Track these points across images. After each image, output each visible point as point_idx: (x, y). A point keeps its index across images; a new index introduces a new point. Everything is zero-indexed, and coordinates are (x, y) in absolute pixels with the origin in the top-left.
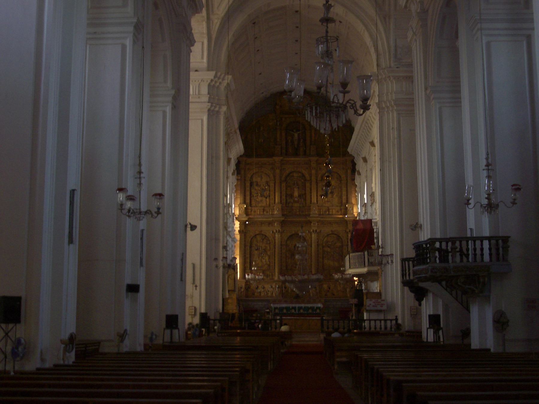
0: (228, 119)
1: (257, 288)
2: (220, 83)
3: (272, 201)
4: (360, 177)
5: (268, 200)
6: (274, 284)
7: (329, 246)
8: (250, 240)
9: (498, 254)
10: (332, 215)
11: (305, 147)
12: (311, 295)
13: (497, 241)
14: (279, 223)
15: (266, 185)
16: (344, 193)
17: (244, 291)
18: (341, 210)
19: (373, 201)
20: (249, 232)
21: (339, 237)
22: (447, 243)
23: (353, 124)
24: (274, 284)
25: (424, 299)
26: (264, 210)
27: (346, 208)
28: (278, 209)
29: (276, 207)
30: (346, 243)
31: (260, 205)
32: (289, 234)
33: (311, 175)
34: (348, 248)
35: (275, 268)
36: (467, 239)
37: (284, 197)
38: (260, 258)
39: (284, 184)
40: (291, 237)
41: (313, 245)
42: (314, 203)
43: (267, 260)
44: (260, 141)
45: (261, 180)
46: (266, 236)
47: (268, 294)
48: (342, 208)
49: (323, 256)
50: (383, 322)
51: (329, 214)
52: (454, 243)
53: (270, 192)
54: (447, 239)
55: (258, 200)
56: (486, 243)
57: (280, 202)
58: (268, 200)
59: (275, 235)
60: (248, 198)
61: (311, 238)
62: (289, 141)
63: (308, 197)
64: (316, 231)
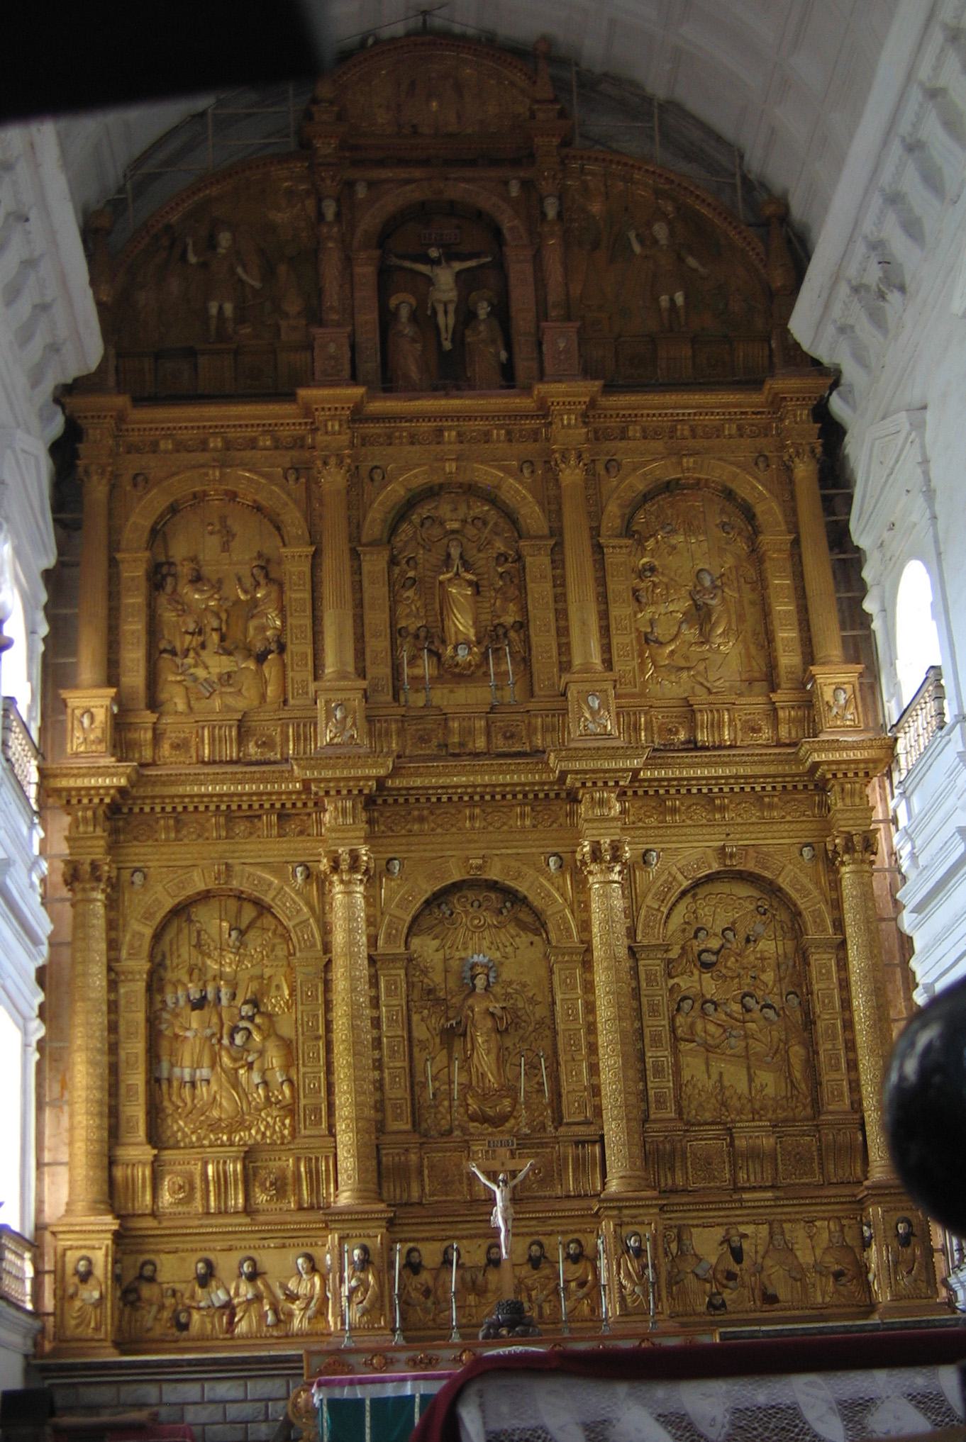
1: (205, 1279)
3: (300, 673)
6: (332, 1239)
7: (705, 957)
8: (148, 932)
10: (720, 747)
11: (509, 347)
14: (349, 804)
16: (783, 607)
17: (102, 1297)
18: (773, 713)
20: (138, 878)
21: (772, 889)
24: (332, 1239)
26: (243, 731)
27: (808, 704)
28: (345, 718)
29: (328, 702)
30: (831, 931)
31: (217, 703)
32: (428, 889)
33: (553, 506)
34: (843, 965)
35: (331, 1127)
37: (378, 645)
38: (226, 1060)
39: (375, 563)
41: (598, 953)
42: (587, 668)
43: (279, 1078)
44: (214, 310)
45: (225, 547)
46: (262, 908)
47: (290, 1315)
49: (673, 1030)
51: (693, 745)
53: (283, 622)
55: (201, 673)
57: (351, 669)
58: (270, 669)
59: (324, 894)
60: (134, 657)
61: (582, 906)
62: (404, 313)
63: (543, 640)
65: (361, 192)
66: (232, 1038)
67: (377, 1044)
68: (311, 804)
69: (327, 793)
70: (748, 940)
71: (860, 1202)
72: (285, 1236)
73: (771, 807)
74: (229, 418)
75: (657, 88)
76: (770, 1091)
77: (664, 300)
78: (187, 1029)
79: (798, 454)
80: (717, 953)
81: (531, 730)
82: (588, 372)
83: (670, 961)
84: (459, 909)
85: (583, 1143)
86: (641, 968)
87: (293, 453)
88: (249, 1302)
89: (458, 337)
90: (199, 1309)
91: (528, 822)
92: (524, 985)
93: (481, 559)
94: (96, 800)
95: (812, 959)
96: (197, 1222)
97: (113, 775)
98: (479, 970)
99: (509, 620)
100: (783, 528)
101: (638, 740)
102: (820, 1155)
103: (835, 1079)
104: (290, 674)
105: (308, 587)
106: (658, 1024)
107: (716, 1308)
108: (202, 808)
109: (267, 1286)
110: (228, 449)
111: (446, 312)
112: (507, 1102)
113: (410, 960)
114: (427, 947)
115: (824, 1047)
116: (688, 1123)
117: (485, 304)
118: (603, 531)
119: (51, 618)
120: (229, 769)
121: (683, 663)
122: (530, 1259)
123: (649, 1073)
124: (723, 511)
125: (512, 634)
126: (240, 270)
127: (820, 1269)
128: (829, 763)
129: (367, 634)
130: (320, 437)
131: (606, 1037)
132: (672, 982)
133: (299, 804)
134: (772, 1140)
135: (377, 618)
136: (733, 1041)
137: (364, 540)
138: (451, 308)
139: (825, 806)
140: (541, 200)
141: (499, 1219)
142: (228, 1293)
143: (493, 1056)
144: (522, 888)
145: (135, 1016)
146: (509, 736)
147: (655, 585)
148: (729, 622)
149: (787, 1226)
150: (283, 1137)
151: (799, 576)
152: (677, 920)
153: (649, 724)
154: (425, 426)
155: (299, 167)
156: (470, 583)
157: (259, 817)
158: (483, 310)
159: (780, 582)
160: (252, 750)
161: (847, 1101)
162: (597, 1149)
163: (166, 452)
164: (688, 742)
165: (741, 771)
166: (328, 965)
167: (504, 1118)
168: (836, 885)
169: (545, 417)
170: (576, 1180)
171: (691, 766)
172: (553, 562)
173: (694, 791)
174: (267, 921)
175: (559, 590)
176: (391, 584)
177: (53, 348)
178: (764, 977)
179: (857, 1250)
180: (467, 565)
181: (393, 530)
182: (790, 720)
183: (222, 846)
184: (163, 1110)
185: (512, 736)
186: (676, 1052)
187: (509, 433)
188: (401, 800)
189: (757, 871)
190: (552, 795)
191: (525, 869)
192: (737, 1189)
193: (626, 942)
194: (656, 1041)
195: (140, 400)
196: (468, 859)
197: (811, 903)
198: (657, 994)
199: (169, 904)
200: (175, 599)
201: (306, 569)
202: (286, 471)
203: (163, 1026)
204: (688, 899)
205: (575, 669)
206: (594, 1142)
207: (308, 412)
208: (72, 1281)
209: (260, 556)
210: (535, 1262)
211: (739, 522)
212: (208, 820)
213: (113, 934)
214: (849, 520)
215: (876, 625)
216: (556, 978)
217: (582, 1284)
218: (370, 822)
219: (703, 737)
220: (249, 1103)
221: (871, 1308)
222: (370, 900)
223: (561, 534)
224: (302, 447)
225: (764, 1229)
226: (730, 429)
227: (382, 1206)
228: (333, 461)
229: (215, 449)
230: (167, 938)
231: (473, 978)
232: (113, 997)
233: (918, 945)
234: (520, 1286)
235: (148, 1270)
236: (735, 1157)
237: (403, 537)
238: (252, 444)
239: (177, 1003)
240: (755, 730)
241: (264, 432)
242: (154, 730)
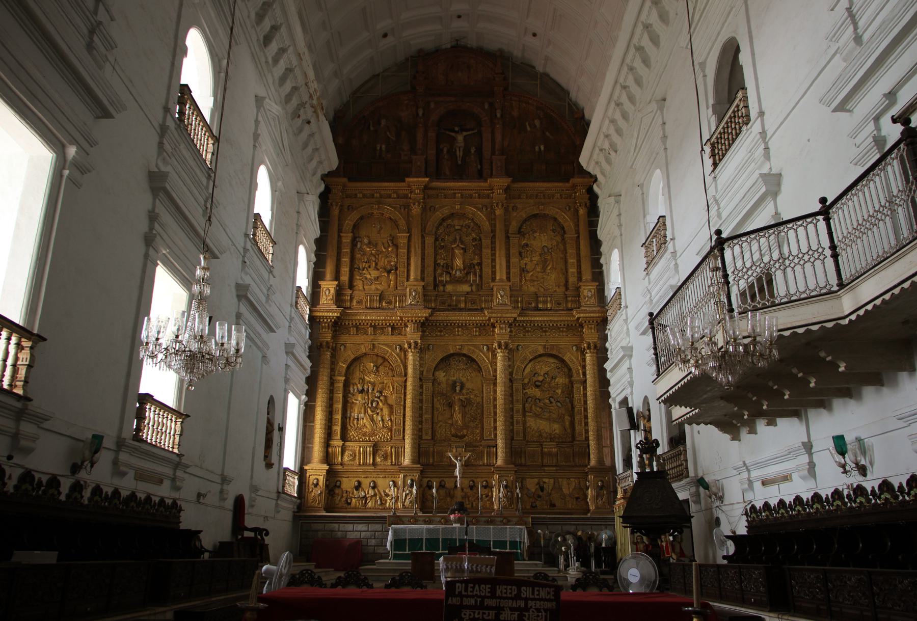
5: (392, 277)
7: (537, 383)
8: (345, 366)
10: (547, 310)
11: (481, 165)
12: (496, 507)
15: (390, 242)
16: (572, 261)
20: (342, 348)
21: (562, 361)
24: (401, 476)
26: (382, 297)
28: (416, 295)
32: (441, 356)
34: (585, 388)
35: (404, 436)
37: (430, 270)
40: (446, 361)
41: (499, 380)
42: (501, 280)
44: (378, 148)
45: (379, 232)
46: (385, 359)
47: (386, 501)
49: (524, 408)
51: (537, 309)
55: (368, 276)
57: (419, 278)
58: (392, 277)
59: (405, 355)
60: (345, 270)
61: (494, 363)
62: (445, 150)
63: (487, 270)
64: (507, 345)
65: (432, 105)
66: (372, 404)
67: (421, 408)
68: (403, 324)
69: (408, 321)
70: (552, 378)
71: (587, 473)
72: (386, 474)
73: (562, 331)
74: (380, 187)
75: (540, 69)
76: (557, 431)
77: (537, 148)
78: (357, 400)
79: (580, 206)
80: (541, 382)
81: (481, 301)
82: (508, 174)
83: (525, 384)
84: (452, 363)
85: (490, 447)
86: (514, 386)
87: (405, 200)
88: (372, 496)
90: (355, 498)
91: (477, 334)
92: (473, 390)
93: (467, 240)
94: (329, 320)
95: (575, 386)
96: (356, 468)
97: (335, 312)
98: (458, 384)
99: (475, 262)
100: (574, 232)
101: (518, 306)
102: (573, 456)
103: (579, 428)
104: (398, 278)
105: (406, 248)
107: (533, 507)
108: (366, 324)
109: (379, 491)
110: (381, 198)
111: (460, 151)
112: (465, 431)
113: (434, 380)
114: (441, 375)
115: (577, 418)
116: (528, 441)
117: (474, 148)
118: (510, 232)
119: (317, 255)
120: (375, 311)
121: (535, 279)
122: (470, 486)
123: (515, 423)
124: (553, 225)
125: (476, 267)
126: (388, 133)
128: (583, 317)
129: (426, 265)
130: (413, 195)
132: (524, 391)
133: (399, 324)
134: (556, 450)
135: (430, 261)
136: (545, 414)
137: (426, 232)
138: (461, 149)
139: (581, 331)
140: (496, 110)
141: (457, 473)
142: (365, 492)
143: (461, 414)
144: (474, 357)
145: (339, 396)
146: (473, 302)
147: (528, 251)
148: (553, 265)
149: (560, 480)
150: (387, 439)
151: (578, 249)
152: (527, 370)
153: (522, 301)
154: (450, 192)
156: (463, 249)
157: (385, 328)
158: (473, 150)
159: (571, 251)
160: (384, 304)
161: (584, 437)
162: (495, 449)
163: (360, 198)
164: (535, 307)
165: (553, 319)
166: (406, 381)
167: (464, 436)
168: (584, 360)
169: (492, 190)
170: (487, 459)
171: (535, 316)
172: (492, 242)
173: (536, 325)
175: (493, 252)
176: (435, 247)
177: (320, 162)
178: (557, 391)
179: (585, 490)
180: (462, 242)
181: (438, 228)
182: (572, 301)
183: (372, 337)
184: (347, 428)
185: (474, 303)
186: (524, 416)
187: (479, 195)
188: (434, 324)
189: (557, 354)
190: (486, 324)
191: (475, 350)
192: (543, 466)
193: (509, 377)
195: (351, 180)
196: (455, 346)
197: (576, 367)
198: (518, 396)
199: (353, 357)
200: (361, 249)
201: (406, 241)
202: (401, 206)
203: (349, 399)
204: (533, 362)
205: (496, 281)
206: (493, 447)
207: (409, 186)
209: (391, 235)
210: (471, 488)
212: (368, 328)
213: (333, 366)
214: (597, 230)
215: (604, 268)
216: (484, 388)
217: (487, 496)
218: (423, 331)
219: (540, 306)
220: (377, 427)
221: (589, 510)
222: (421, 358)
223: (495, 232)
224: (407, 198)
225: (552, 481)
226: (557, 196)
227: (419, 466)
228: (417, 204)
229: (377, 198)
230: (352, 368)
231: (456, 387)
232: (332, 388)
233: (611, 382)
234: (466, 496)
235: (338, 483)
236: (542, 453)
237: (441, 231)
238: (390, 196)
239: (354, 391)
240: (559, 304)
241: (394, 193)
242: (351, 296)
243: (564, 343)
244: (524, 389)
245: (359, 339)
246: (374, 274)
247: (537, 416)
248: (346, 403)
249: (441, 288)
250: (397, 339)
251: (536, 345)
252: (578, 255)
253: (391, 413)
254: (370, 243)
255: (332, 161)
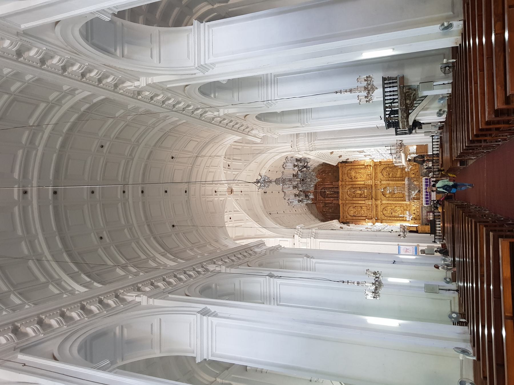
0: (320, 228)
1: (415, 214)
2: (300, 232)
3: (364, 205)
4: (350, 159)
5: (363, 207)
8: (386, 217)
9: (393, 83)
10: (371, 173)
13: (385, 84)
16: (359, 167)
19: (363, 152)
22: (387, 111)
23: (321, 163)
24: (412, 204)
25: (419, 121)
31: (366, 212)
32: (383, 196)
34: (390, 164)
36: (385, 100)
37: (361, 199)
39: (354, 199)
43: (398, 208)
45: (352, 211)
46: (384, 208)
48: (367, 167)
49: (395, 177)
50: (433, 144)
51: (371, 175)
52: (387, 107)
54: (384, 111)
55: (363, 213)
56: (387, 90)
58: (363, 207)
60: (362, 218)
63: (361, 186)
65: (319, 199)
67: (396, 200)
89: (333, 191)
99: (359, 189)
106: (395, 179)
114: (387, 196)
116: (403, 176)
127: (415, 167)
131: (396, 183)
135: (359, 199)
146: (369, 189)
151: (355, 165)
155: (317, 204)
159: (356, 167)
168: (383, 164)
174: (385, 208)
194: (396, 179)
197: (385, 166)
198: (392, 179)
199: (384, 216)
208: (415, 223)
211: (350, 170)
218: (377, 200)
219: (370, 174)
243: (379, 169)
244: (390, 177)
245: (379, 214)
246: (362, 211)
247: (397, 174)
248: (394, 217)
249: (366, 196)
250: (379, 206)
251: (380, 175)
252: (357, 165)
253: (397, 207)
254: (355, 213)
255: (337, 220)
